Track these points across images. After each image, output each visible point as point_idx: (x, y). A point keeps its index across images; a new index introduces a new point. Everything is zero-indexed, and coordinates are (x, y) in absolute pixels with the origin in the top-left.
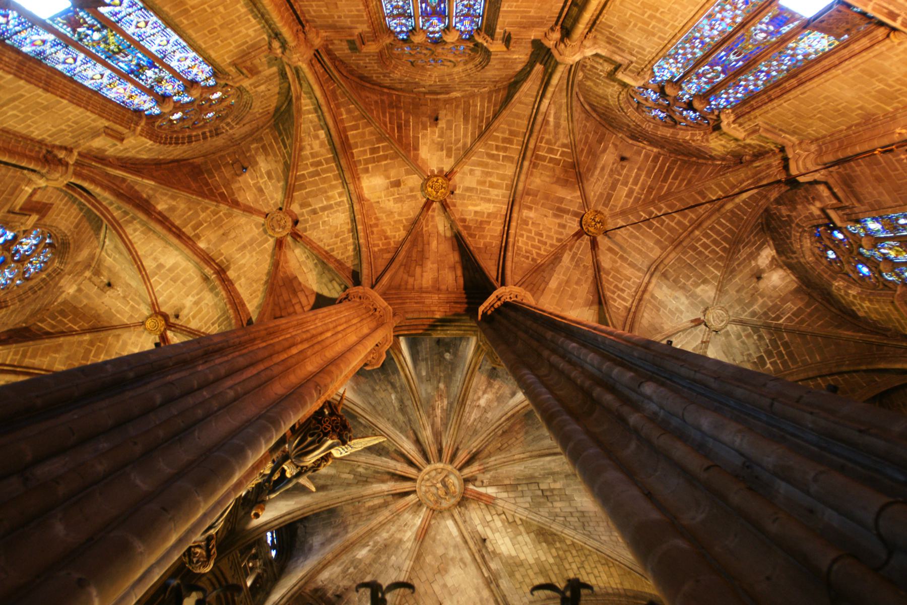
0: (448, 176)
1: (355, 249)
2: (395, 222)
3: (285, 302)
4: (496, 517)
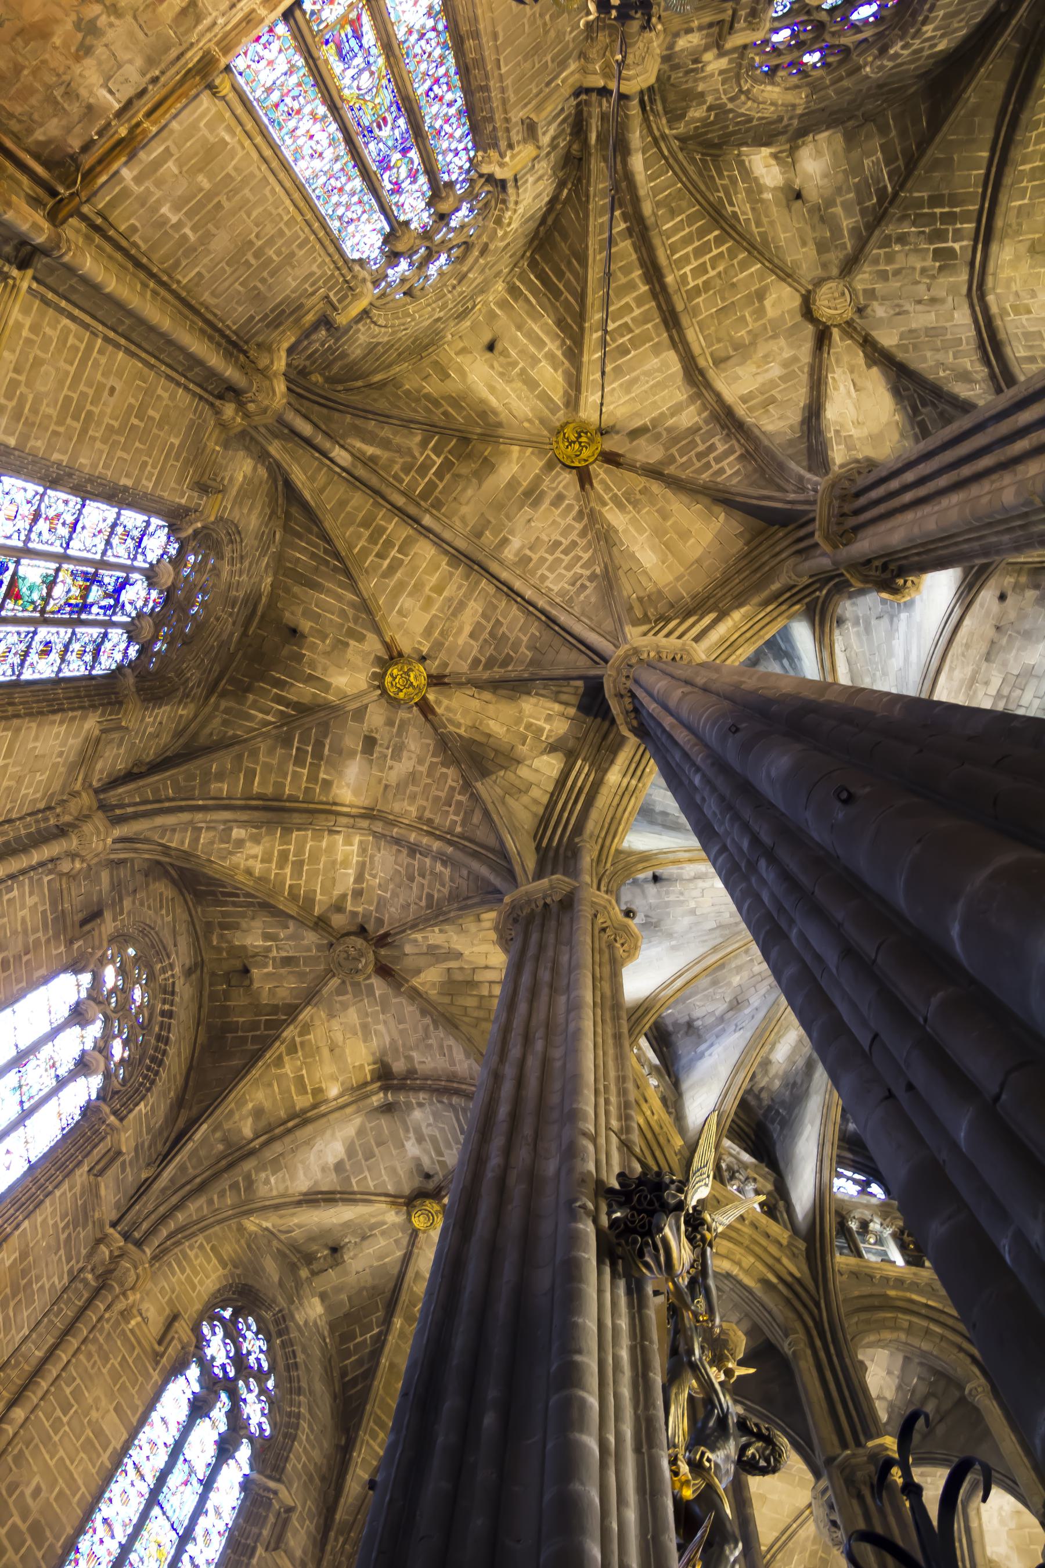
2: (429, 775)
3: (479, 1007)
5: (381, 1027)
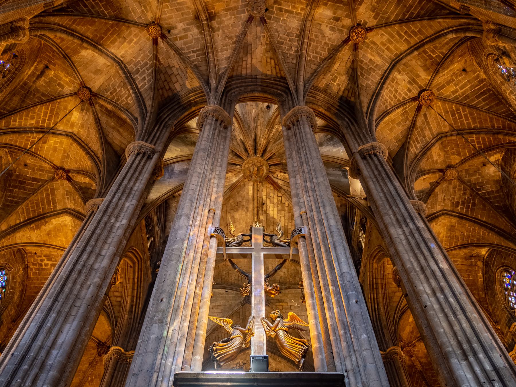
0: (369, 30)
1: (297, 51)
4: (276, 197)
5: (228, 17)
